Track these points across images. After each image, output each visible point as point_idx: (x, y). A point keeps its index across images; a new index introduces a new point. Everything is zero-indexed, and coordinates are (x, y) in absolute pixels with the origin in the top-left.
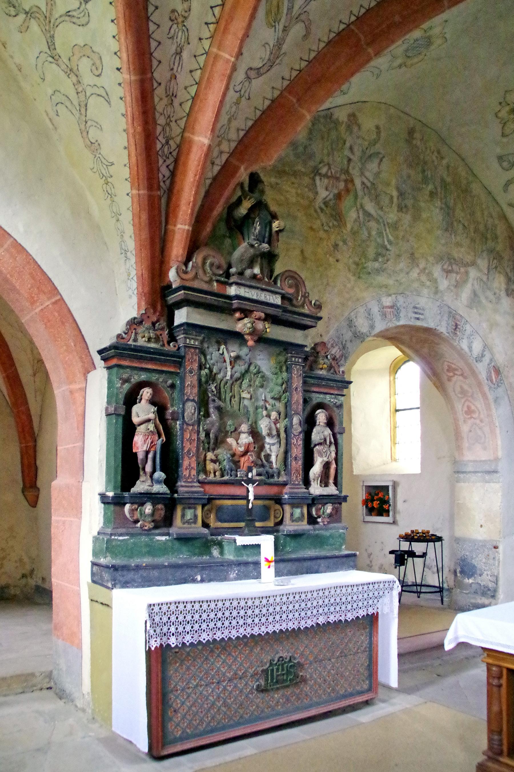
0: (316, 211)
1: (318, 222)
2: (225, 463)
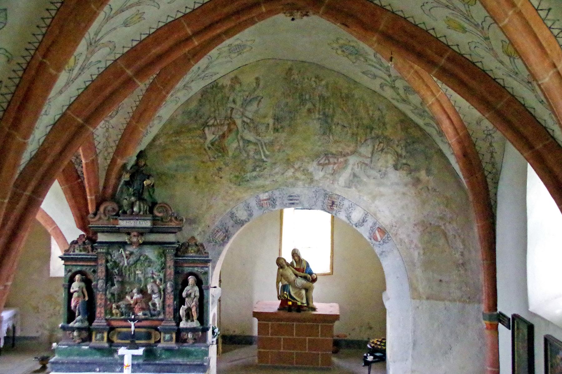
0: (205, 149)
1: (207, 157)
2: (123, 309)
